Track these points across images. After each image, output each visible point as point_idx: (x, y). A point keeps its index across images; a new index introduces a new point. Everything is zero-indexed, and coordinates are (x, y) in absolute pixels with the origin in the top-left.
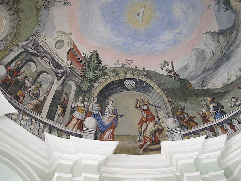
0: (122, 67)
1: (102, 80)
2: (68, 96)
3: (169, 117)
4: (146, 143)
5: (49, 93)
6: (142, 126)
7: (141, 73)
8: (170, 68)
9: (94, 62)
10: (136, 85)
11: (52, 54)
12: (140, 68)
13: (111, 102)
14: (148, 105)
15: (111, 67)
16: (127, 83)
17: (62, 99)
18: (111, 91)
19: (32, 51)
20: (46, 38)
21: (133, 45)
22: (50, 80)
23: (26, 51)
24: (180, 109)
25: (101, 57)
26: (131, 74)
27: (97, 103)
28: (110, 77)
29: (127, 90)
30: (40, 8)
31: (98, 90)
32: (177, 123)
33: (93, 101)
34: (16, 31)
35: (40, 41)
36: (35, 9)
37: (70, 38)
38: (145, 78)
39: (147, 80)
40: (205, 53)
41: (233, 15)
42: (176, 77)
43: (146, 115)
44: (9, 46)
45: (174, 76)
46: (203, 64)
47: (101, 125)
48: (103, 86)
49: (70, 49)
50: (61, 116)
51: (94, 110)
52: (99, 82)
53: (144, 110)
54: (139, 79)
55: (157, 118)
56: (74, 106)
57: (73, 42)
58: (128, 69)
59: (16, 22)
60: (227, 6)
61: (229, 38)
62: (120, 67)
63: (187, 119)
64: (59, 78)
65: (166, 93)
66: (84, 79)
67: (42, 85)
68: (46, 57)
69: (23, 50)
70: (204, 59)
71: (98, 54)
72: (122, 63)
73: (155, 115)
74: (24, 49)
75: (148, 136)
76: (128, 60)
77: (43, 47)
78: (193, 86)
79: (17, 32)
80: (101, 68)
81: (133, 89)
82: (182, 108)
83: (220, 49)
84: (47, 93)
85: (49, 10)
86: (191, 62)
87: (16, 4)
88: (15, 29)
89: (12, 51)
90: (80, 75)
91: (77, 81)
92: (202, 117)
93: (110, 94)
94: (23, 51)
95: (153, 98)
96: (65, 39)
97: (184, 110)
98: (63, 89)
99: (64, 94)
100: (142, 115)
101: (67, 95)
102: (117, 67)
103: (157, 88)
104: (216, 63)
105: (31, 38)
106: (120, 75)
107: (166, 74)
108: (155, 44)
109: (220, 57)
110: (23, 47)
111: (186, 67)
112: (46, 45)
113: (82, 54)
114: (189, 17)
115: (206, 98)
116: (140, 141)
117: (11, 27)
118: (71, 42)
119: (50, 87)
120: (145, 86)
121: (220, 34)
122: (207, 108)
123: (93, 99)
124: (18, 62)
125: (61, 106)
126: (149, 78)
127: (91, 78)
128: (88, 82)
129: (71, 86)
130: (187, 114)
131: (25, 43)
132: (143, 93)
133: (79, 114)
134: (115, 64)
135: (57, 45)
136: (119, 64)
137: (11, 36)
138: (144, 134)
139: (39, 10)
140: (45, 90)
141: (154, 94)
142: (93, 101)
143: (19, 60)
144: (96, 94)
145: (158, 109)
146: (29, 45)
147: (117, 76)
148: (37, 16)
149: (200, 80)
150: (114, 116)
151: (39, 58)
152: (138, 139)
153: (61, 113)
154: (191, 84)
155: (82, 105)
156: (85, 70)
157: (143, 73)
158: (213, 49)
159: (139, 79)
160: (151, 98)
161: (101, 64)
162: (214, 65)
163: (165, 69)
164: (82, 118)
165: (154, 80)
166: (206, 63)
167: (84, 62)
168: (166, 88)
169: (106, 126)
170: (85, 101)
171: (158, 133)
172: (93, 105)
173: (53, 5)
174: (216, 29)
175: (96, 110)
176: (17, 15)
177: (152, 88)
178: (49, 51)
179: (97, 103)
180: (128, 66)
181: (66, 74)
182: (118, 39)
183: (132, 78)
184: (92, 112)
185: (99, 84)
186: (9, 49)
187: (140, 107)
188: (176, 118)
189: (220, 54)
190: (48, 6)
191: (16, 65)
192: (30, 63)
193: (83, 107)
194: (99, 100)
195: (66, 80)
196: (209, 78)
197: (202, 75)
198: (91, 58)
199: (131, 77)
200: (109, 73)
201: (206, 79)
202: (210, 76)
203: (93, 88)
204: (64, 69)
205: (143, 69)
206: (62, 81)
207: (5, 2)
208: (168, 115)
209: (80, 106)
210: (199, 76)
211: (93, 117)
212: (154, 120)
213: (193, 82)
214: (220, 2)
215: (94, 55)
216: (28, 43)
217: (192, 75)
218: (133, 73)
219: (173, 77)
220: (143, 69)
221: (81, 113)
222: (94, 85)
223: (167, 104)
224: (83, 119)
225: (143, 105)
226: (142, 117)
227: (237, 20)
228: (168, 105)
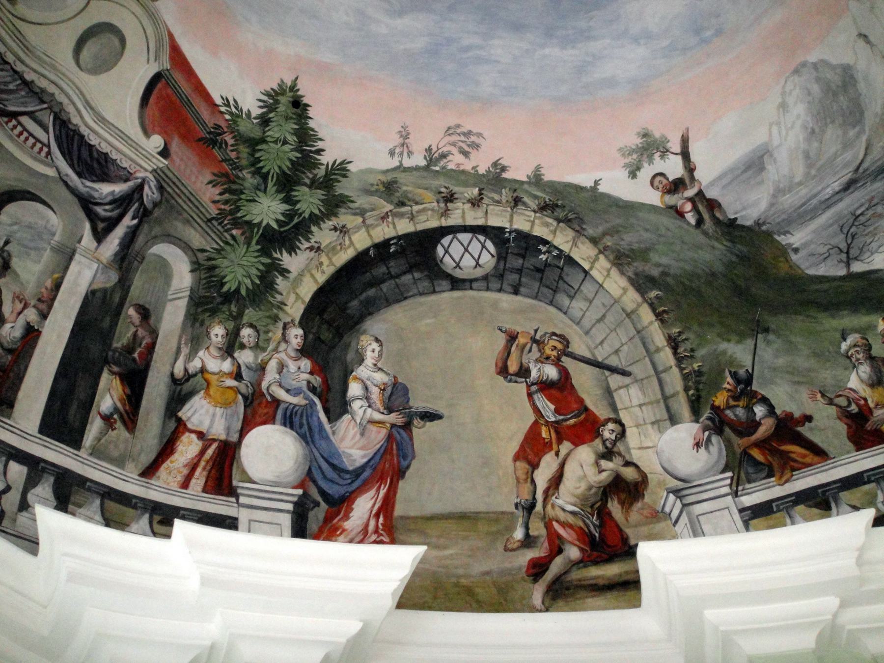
0: (427, 168)
1: (323, 235)
2: (152, 321)
3: (673, 420)
4: (560, 551)
5: (50, 307)
6: (535, 466)
7: (526, 199)
8: (674, 168)
9: (285, 142)
10: (501, 257)
12: (518, 172)
13: (375, 345)
14: (564, 359)
15: (370, 171)
16: (456, 250)
17: (122, 338)
18: (371, 292)
21: (482, 53)
22: (54, 234)
24: (729, 379)
25: (318, 120)
26: (475, 203)
27: (304, 352)
28: (368, 222)
29: (456, 284)
31: (307, 290)
32: (714, 449)
33: (283, 346)
38: (547, 225)
39: (554, 232)
40: (862, 86)
42: (706, 216)
43: (557, 411)
45: (695, 208)
46: (846, 145)
47: (325, 465)
48: (331, 263)
50: (119, 424)
51: (288, 391)
52: (311, 249)
53: (545, 386)
54: (516, 231)
55: (611, 426)
56: (186, 370)
57: (171, 36)
58: (460, 176)
62: (417, 168)
63: (766, 427)
64: (101, 226)
65: (657, 297)
66: (234, 232)
67: (15, 263)
71: (305, 100)
72: (429, 150)
73: (601, 411)
75: (571, 519)
76: (458, 131)
77: (10, 58)
78: (794, 257)
80: (321, 172)
81: (485, 278)
82: (742, 372)
84: (43, 307)
86: (784, 132)
90: (214, 211)
91: (197, 239)
92: (845, 415)
93: (370, 309)
95: (587, 323)
97: (749, 380)
98: (124, 284)
99: (132, 312)
100: (537, 410)
101: (145, 313)
102: (400, 168)
103: (609, 271)
106: (418, 212)
107: (654, 198)
108: (594, 46)
112: (27, 48)
113: (219, 101)
115: (863, 320)
116: (528, 541)
119: (56, 276)
120: (546, 264)
122: (873, 367)
123: (284, 335)
125: (116, 369)
126: (567, 221)
127: (268, 225)
128: (255, 247)
129: (164, 269)
130: (765, 400)
132: (536, 298)
133: (211, 409)
134: (392, 153)
135: (85, 54)
136: (410, 153)
138: (549, 507)
140: (30, 291)
141: (591, 302)
142: (283, 346)
144: (295, 310)
145: (615, 380)
147: (402, 215)
149: (831, 225)
150: (394, 418)
152: (519, 534)
153: (116, 410)
154: (783, 251)
155: (227, 366)
156: (234, 187)
157: (536, 197)
159: (515, 226)
160: (578, 323)
161: (319, 151)
164: (228, 430)
165: (590, 231)
166: (864, 138)
167: (231, 142)
168: (655, 272)
169: (351, 468)
170: (242, 347)
171: (622, 503)
172: (281, 367)
175: (296, 392)
177: (582, 275)
178: (43, 83)
179: (304, 352)
180: (455, 161)
181: (136, 205)
183: (480, 222)
184: (277, 402)
185: (313, 254)
187: (524, 372)
188: (709, 423)
193: (230, 375)
194: (311, 336)
195: (141, 240)
197: (841, 200)
198: (265, 121)
199: (474, 218)
200: (362, 201)
203: (279, 280)
204: (127, 180)
205: (537, 179)
206: (117, 242)
208: (668, 409)
209: (216, 370)
210: (829, 207)
211: (282, 428)
212: (598, 435)
213: (796, 238)
215: (281, 108)
217: (789, 201)
218: (486, 201)
219: (691, 218)
220: (537, 179)
221: (226, 405)
222: (287, 260)
223: (662, 354)
224: (234, 438)
225: (538, 361)
226: (536, 424)
228: (666, 357)
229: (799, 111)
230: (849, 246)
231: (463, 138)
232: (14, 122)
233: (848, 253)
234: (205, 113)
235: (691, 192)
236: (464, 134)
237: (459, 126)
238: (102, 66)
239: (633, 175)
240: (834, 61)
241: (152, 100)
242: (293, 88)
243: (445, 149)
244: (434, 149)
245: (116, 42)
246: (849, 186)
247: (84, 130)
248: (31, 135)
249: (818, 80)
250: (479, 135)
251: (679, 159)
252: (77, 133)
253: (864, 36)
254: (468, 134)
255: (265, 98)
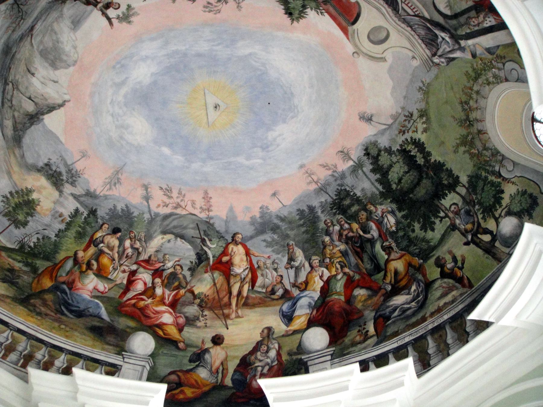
8: (111, 13)
11: (395, 19)
19: (443, 35)
20: (410, 54)
21: (212, 44)
23: (456, 38)
30: (421, 116)
34: (473, 85)
35: (423, 51)
36: (430, 118)
37: (356, 46)
40: (46, 65)
41: (30, 160)
44: (493, 62)
46: (41, 42)
49: (354, 23)
57: (348, 39)
59: (472, 103)
60: (50, 172)
61: (14, 116)
68: (409, 15)
69: (463, 43)
70: (44, 54)
71: (287, 16)
74: (459, 44)
76: (215, 12)
77: (416, 37)
79: (472, 82)
83: (20, 88)
85: (403, 108)
86: (70, 38)
87: (470, 138)
88: (476, 88)
89: (489, 50)
94: (462, 40)
96: (367, 46)
104: (14, 55)
105: (443, 60)
108: (164, 52)
109: (12, 71)
110: (462, 49)
111: (76, 23)
112: (409, 40)
113: (326, 14)
114: (114, 122)
117: (485, 98)
118: (353, 37)
121: (37, 114)
124: (476, 22)
131: (458, 54)
137: (487, 80)
139: (423, 114)
143: (475, 26)
146: (449, 47)
148: (427, 103)
149: (31, 13)
151: (427, 15)
158: (34, 80)
162: (15, 52)
163: (123, 8)
166: (35, 47)
173: (395, 118)
174: (49, 120)
176: (468, 116)
178: (403, 25)
182: (247, 51)
186: (495, 56)
189: (15, 76)
190: (404, 118)
191: (481, 18)
192: (448, 12)
196: (12, 23)
198: (304, 7)
201: (19, 19)
202: (12, 28)
207: (490, 151)
210: (36, 19)
214: (67, 172)
215: (297, 12)
216: (450, 52)
217: (54, 14)
227: (18, 155)
229: (68, 48)
230: (19, 7)
231: (212, 9)
232: (416, 13)
233: (18, 5)
234: (331, 9)
235: (100, 5)
236: (212, 11)
237: (215, 14)
238: (377, 29)
239: (129, 6)
240: (62, 70)
241: (355, 15)
242: (293, 20)
243: (219, 4)
244: (224, 3)
245: (371, 37)
246: (32, 28)
247: (386, 6)
248: (409, 7)
249: (65, 61)
250: (205, 11)
251: (111, 16)
252: (389, 6)
253: (55, 82)
254: (210, 11)
255: (305, 16)
